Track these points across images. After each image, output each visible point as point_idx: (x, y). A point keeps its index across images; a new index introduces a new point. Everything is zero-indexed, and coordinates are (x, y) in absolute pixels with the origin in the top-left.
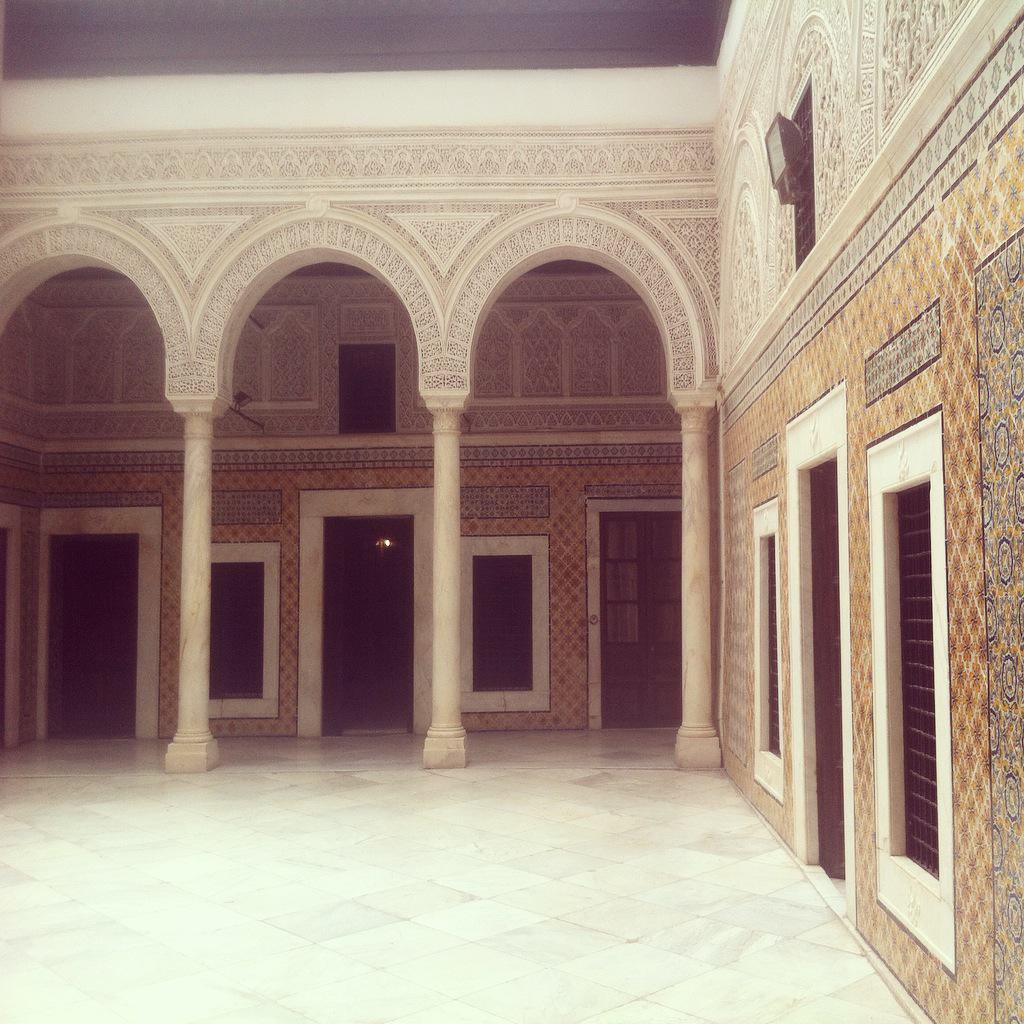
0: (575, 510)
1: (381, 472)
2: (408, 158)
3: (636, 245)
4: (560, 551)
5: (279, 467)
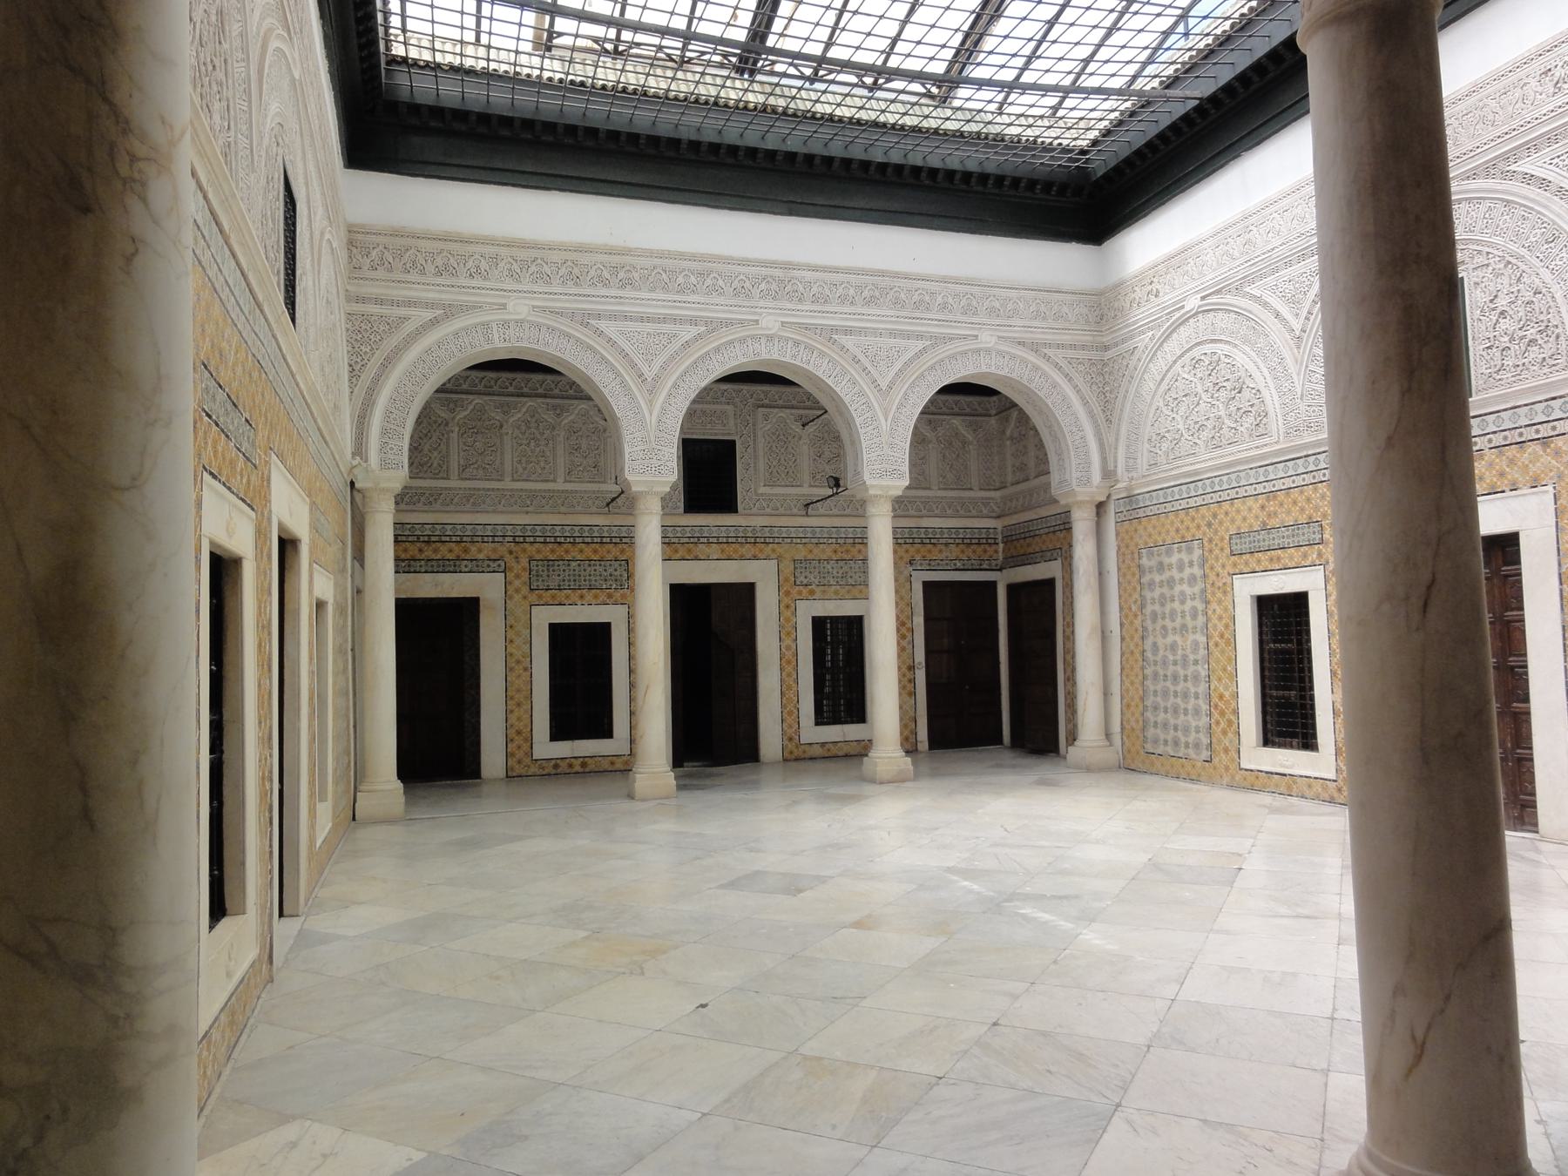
2: (852, 292)
3: (1044, 374)
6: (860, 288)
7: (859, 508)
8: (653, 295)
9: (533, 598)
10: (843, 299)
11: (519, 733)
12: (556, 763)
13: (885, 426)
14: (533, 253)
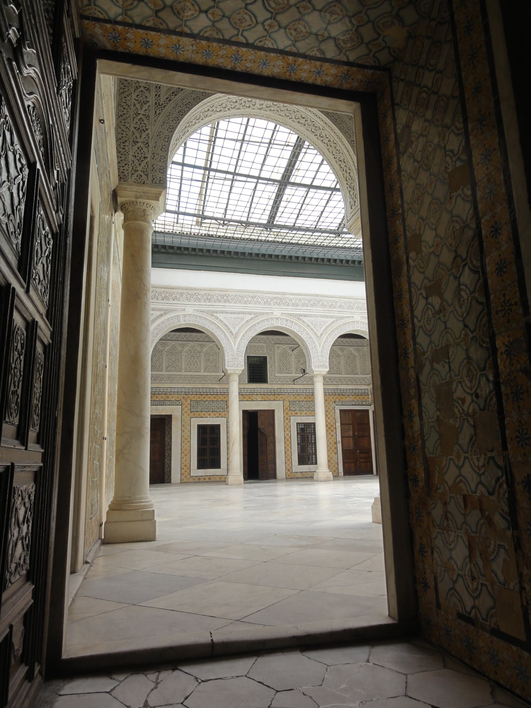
0: (331, 408)
2: (306, 302)
6: (309, 301)
7: (312, 379)
8: (236, 305)
9: (191, 415)
10: (303, 305)
12: (199, 477)
13: (319, 349)
14: (194, 292)
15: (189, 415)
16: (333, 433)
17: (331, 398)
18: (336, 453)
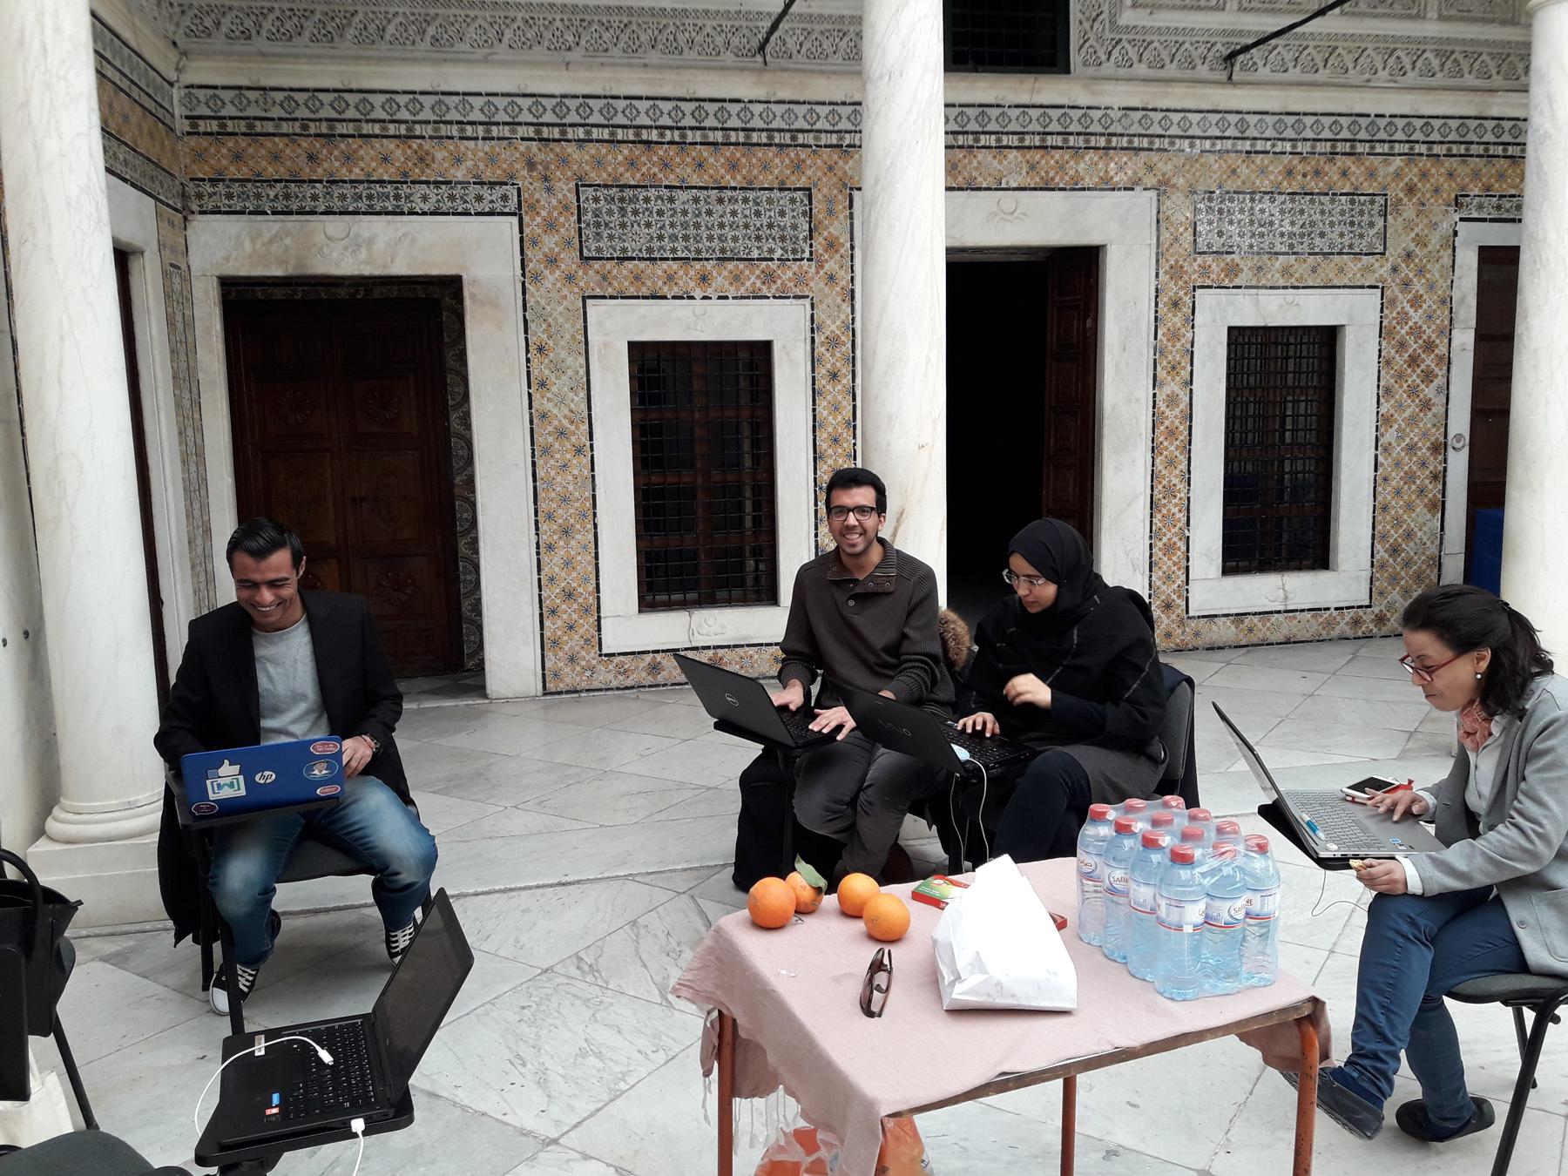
0: (1435, 240)
1: (1038, 155)
4: (1404, 318)
5: (801, 138)
9: (589, 279)
11: (569, 595)
15: (570, 278)
16: (1429, 391)
17: (1437, 174)
18: (1440, 506)
